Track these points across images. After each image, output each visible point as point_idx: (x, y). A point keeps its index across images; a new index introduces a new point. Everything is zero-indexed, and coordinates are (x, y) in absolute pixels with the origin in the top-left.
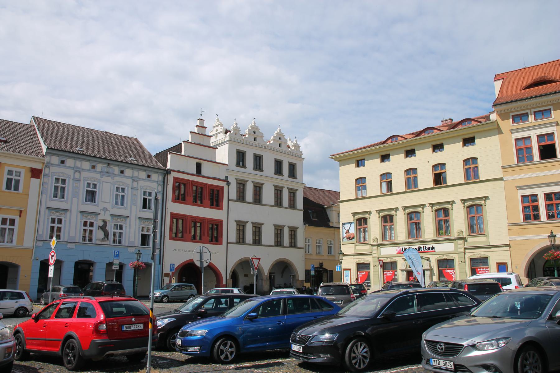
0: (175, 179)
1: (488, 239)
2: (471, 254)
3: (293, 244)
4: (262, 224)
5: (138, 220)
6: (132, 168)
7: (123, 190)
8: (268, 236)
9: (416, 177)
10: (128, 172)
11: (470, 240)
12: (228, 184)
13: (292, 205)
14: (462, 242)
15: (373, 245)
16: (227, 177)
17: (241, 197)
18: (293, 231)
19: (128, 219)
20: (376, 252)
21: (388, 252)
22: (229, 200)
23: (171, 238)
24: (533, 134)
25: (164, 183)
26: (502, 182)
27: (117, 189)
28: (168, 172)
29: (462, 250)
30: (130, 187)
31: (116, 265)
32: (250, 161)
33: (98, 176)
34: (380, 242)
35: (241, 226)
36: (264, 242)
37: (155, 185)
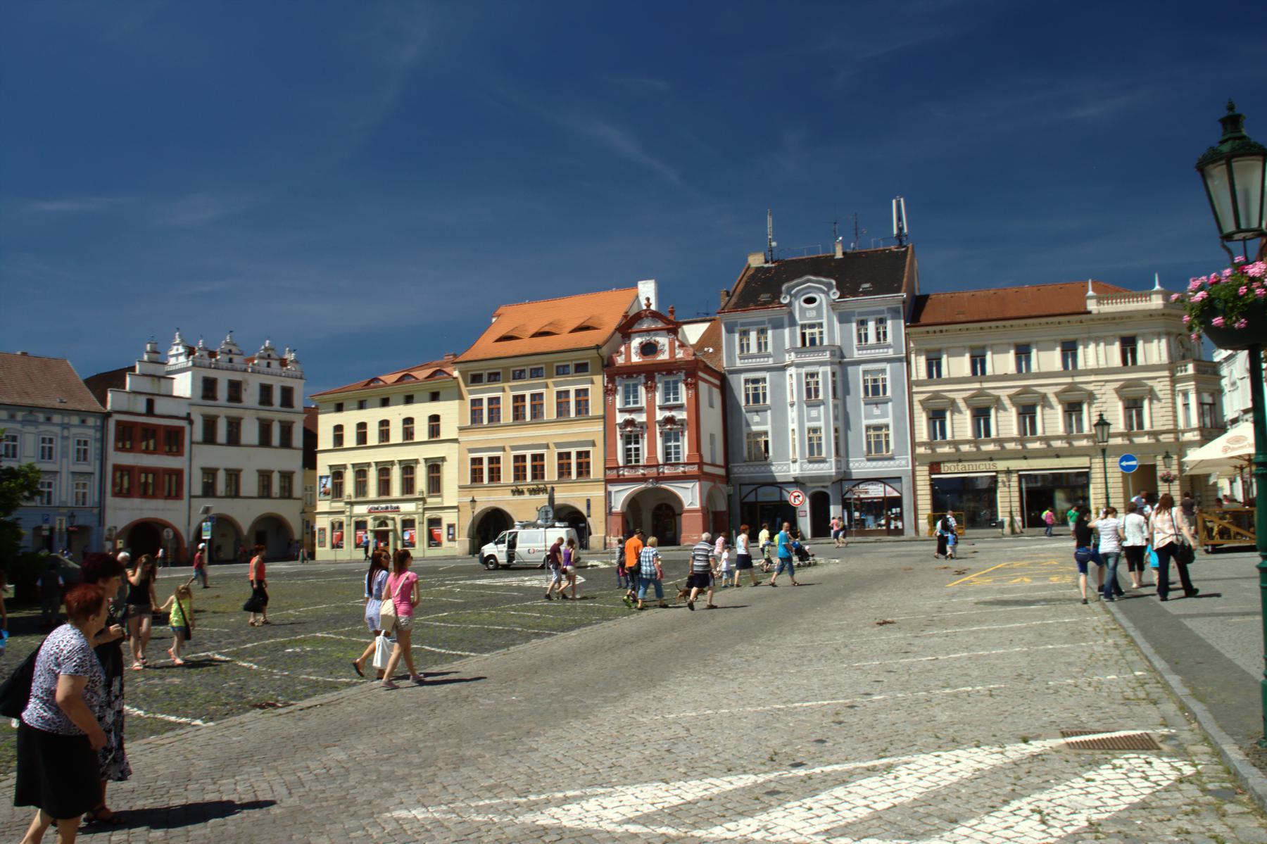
0: (118, 423)
1: (442, 500)
2: (428, 515)
3: (287, 493)
4: (240, 471)
5: (70, 476)
6: (61, 414)
7: (51, 441)
8: (249, 484)
9: (388, 431)
10: (57, 418)
11: (429, 500)
12: (191, 422)
13: (286, 443)
14: (421, 503)
15: (347, 503)
16: (189, 414)
17: (209, 438)
18: (287, 477)
19: (58, 475)
20: (348, 510)
21: (360, 510)
22: (192, 443)
23: (115, 495)
24: (485, 397)
25: (103, 429)
26: (456, 445)
27: (44, 440)
28: (109, 415)
29: (421, 510)
30: (60, 435)
31: (46, 530)
32: (222, 391)
33: (18, 426)
34: (353, 499)
35: (210, 473)
36: (243, 492)
37: (91, 432)
